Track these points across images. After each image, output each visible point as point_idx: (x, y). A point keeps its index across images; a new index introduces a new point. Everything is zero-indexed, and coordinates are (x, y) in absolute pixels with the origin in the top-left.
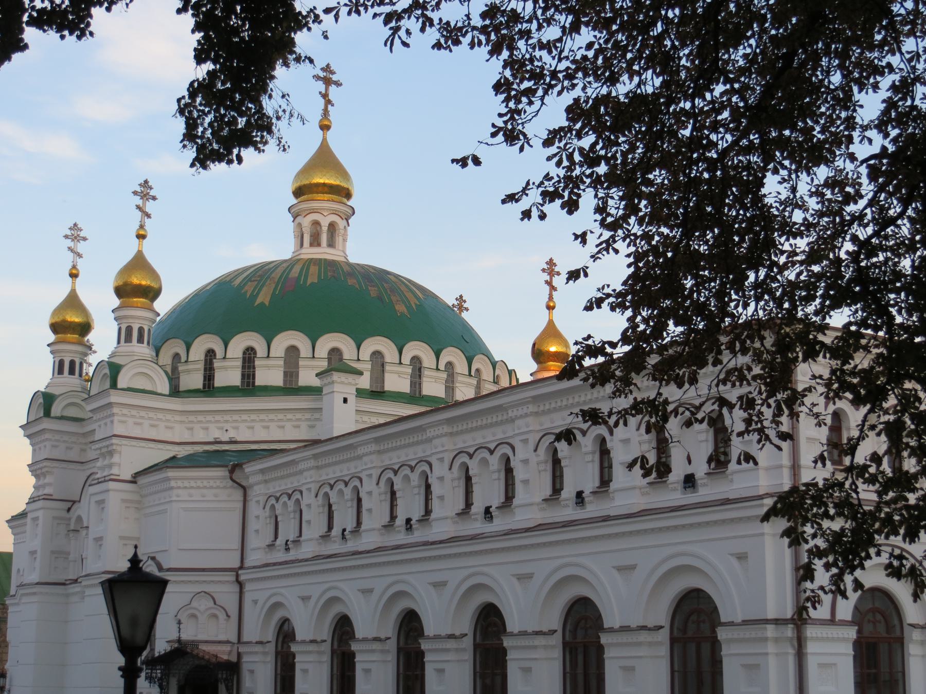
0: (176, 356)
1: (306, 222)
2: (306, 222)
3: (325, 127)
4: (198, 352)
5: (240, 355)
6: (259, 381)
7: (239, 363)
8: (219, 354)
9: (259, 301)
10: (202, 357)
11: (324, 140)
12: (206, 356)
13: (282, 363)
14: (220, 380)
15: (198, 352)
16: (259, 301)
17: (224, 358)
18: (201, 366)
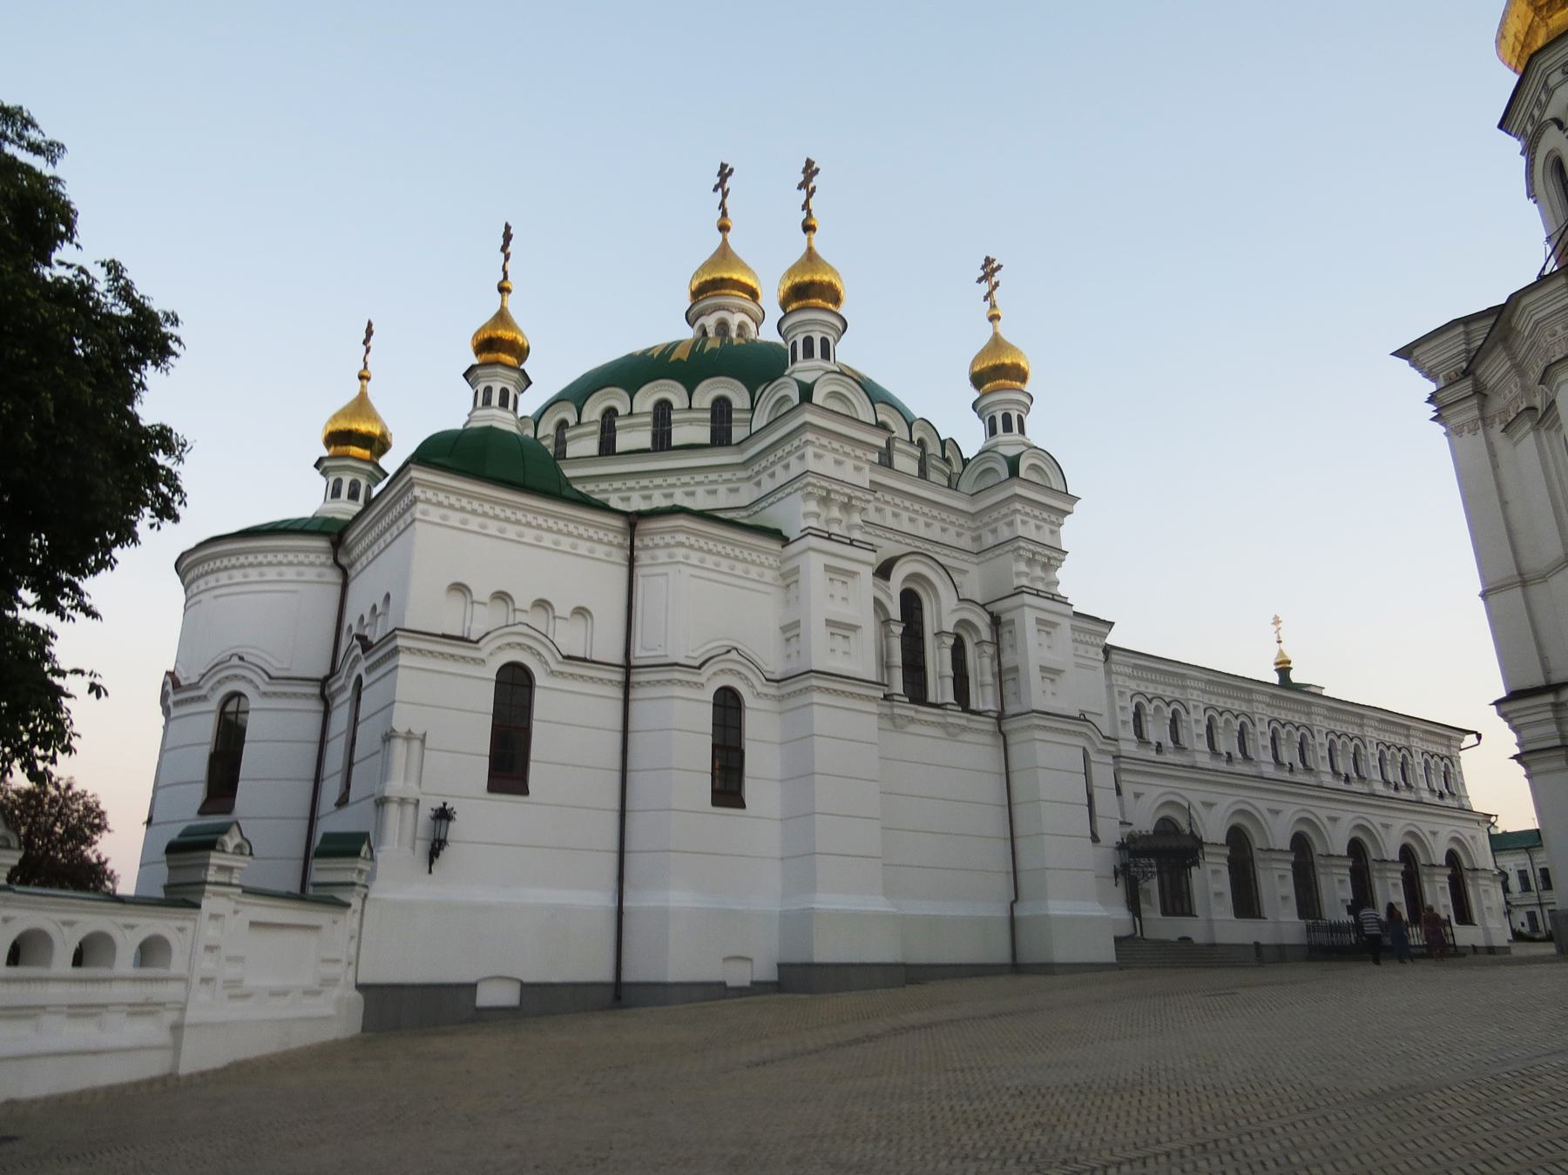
0: (563, 425)
1: (710, 322)
2: (710, 322)
3: (724, 228)
4: (593, 411)
5: (648, 406)
6: (674, 442)
7: (649, 419)
8: (622, 411)
9: (673, 358)
10: (599, 418)
11: (725, 240)
12: (603, 417)
13: (709, 416)
14: (623, 442)
15: (593, 411)
16: (673, 358)
17: (631, 414)
18: (596, 428)
